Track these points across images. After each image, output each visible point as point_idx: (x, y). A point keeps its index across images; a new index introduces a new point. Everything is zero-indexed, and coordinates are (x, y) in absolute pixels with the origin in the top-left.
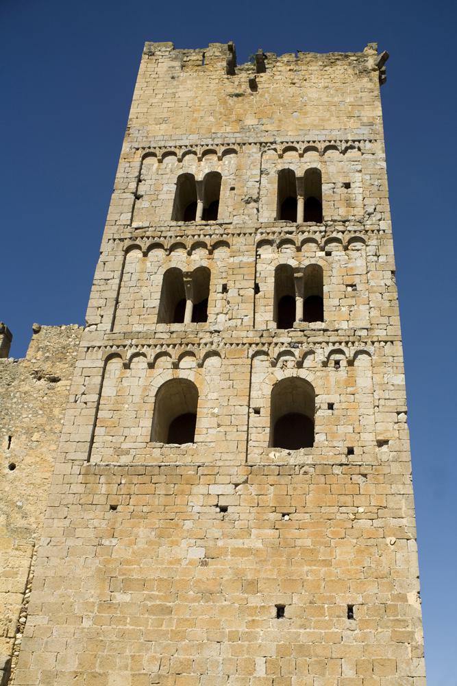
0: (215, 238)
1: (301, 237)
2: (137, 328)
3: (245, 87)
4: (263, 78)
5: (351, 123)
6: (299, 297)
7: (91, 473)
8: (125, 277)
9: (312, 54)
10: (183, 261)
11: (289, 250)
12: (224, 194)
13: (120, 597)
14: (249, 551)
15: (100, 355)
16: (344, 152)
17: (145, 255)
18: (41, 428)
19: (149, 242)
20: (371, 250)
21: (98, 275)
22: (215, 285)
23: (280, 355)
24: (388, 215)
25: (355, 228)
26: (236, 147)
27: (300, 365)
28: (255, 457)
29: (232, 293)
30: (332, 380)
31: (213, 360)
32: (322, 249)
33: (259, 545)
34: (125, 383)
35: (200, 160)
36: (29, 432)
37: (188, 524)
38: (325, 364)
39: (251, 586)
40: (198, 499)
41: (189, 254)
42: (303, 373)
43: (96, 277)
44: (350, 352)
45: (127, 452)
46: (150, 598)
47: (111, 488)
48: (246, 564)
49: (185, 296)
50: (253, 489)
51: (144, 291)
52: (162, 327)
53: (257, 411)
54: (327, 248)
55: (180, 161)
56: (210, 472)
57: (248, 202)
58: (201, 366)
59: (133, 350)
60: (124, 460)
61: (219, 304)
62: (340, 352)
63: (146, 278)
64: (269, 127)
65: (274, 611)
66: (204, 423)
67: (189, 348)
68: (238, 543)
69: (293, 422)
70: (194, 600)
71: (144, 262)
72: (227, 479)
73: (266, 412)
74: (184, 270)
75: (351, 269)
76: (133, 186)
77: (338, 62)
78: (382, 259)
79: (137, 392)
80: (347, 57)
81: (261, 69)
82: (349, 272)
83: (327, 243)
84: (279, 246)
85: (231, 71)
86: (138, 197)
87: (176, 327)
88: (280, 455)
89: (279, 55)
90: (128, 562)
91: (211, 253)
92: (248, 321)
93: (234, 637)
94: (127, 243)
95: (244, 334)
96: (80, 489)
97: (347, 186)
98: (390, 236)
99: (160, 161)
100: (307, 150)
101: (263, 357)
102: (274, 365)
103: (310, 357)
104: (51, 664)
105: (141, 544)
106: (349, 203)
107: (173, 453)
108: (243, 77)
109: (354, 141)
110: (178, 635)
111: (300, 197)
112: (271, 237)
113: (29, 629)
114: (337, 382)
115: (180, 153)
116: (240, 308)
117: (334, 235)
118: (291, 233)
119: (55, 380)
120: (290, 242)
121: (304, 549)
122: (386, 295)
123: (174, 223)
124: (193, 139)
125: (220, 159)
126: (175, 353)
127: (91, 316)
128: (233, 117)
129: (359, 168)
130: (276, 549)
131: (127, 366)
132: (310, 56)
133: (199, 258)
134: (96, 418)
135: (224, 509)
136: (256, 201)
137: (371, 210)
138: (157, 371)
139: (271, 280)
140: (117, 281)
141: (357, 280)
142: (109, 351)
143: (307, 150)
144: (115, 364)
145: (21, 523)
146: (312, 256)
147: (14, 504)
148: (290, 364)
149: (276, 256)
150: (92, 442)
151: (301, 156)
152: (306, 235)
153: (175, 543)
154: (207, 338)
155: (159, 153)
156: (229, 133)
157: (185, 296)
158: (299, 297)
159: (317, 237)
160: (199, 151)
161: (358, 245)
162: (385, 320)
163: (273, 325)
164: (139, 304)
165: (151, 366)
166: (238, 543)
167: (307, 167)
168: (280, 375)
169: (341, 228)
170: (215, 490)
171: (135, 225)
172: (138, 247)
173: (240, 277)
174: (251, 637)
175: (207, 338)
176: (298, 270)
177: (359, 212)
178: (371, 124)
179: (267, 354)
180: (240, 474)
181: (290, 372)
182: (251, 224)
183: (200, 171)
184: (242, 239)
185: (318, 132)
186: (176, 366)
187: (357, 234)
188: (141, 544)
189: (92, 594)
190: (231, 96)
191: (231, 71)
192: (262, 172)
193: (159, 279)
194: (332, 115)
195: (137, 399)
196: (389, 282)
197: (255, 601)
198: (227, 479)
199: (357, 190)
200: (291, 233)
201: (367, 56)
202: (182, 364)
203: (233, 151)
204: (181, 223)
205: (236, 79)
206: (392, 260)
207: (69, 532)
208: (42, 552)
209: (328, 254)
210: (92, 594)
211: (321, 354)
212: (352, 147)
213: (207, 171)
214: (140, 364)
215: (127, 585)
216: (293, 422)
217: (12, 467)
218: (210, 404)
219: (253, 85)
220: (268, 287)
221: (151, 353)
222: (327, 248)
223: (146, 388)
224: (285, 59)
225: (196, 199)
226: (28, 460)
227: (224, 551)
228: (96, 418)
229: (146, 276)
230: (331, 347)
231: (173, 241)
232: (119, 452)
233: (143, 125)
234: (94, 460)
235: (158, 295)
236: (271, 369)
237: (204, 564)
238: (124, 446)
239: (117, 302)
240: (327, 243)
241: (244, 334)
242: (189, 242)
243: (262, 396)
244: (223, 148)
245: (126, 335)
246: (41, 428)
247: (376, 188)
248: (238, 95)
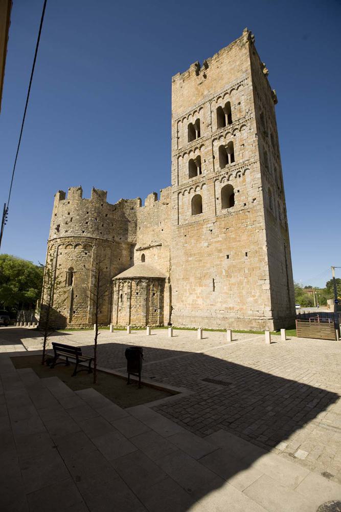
0: (201, 144)
1: (225, 133)
2: (184, 182)
3: (203, 78)
4: (208, 72)
5: (239, 74)
6: (226, 154)
7: (179, 228)
8: (179, 167)
9: (223, 49)
10: (193, 156)
11: (222, 139)
12: (202, 126)
13: (190, 259)
14: (218, 241)
15: (176, 194)
16: (237, 89)
17: (183, 157)
18: (166, 218)
19: (183, 153)
20: (248, 127)
21: (172, 169)
22: (202, 161)
23: (222, 178)
24: (254, 110)
25: (243, 121)
26: (202, 106)
27: (228, 180)
28: (218, 213)
29: (207, 162)
30: (238, 182)
31: (204, 186)
32: (232, 134)
33: (221, 239)
34: (184, 200)
35: (193, 116)
36: (164, 220)
37: (203, 237)
38: (236, 177)
39: (220, 251)
40: (205, 230)
41: (194, 152)
42: (230, 183)
43: (172, 169)
44: (242, 171)
45: (187, 220)
46: (196, 258)
47: (186, 231)
48: (218, 245)
49: (195, 167)
50: (218, 223)
51: (184, 170)
52: (191, 180)
53: (218, 199)
54: (234, 133)
55: (187, 119)
56: (206, 221)
57: (208, 126)
58: (201, 189)
59: (184, 190)
60: (187, 222)
61: (204, 167)
62: (240, 171)
63: (184, 163)
64: (211, 92)
65: (226, 257)
66: (204, 206)
67: (197, 185)
68: (215, 240)
69: (229, 197)
70: (207, 257)
71: (183, 160)
72: (211, 222)
73: (220, 199)
74: (194, 159)
75: (242, 138)
76: (176, 135)
77: (233, 47)
78: (252, 130)
79: (187, 202)
80: (236, 42)
81: (207, 67)
82: (241, 140)
83: (233, 132)
84: (219, 139)
85: (198, 74)
86: (178, 138)
87: (194, 178)
88: (225, 211)
89: (212, 57)
90: (190, 250)
91: (200, 150)
92: (212, 170)
93: (217, 265)
94: (178, 155)
95: (211, 175)
96: (177, 232)
97: (239, 103)
98: (255, 119)
99: (182, 122)
100: (224, 95)
101: (218, 181)
102: (221, 182)
103: (231, 176)
104: (178, 277)
105: (193, 245)
106: (240, 111)
107: (198, 217)
108: (202, 74)
109: (240, 82)
110: (204, 266)
111: (224, 115)
112: (216, 137)
113: (172, 269)
114: (240, 182)
115: (187, 116)
116: (210, 167)
117: (236, 127)
118: (222, 132)
119: (168, 204)
120: (222, 136)
121: (233, 238)
122: (254, 145)
123: (189, 143)
124: (190, 109)
125: (199, 113)
126: (194, 187)
127: (173, 183)
128: (200, 94)
129: (243, 94)
130: (226, 239)
131: (183, 195)
132: (223, 51)
133: (197, 153)
134: (178, 212)
135: (211, 231)
136: (211, 125)
137: (247, 111)
138: (191, 194)
139: (218, 153)
140: (177, 169)
141: (244, 142)
142: (178, 192)
143: (224, 95)
144: (181, 195)
145: (166, 244)
146: (230, 138)
147: (164, 239)
148: (226, 180)
149: (218, 143)
150: (178, 219)
151: (223, 99)
152: (227, 131)
153: (201, 243)
154: (202, 180)
155: (181, 119)
156: (200, 101)
157: (195, 167)
158: (226, 154)
159: (230, 131)
160: (192, 113)
161: (244, 127)
162: (253, 155)
163: (220, 168)
164: (184, 175)
165: (189, 193)
166: (215, 240)
167: (225, 102)
168: (223, 185)
169: (238, 123)
170: (209, 226)
171: (179, 149)
172: (181, 156)
173: (208, 156)
174: (221, 265)
175: (202, 180)
176: (226, 145)
177: (244, 113)
178: (247, 70)
179: (218, 179)
180: (214, 220)
181: (226, 183)
182: (210, 134)
183: (193, 120)
184: (208, 141)
185: (228, 85)
186: (195, 191)
187: (243, 124)
188: (193, 245)
189: (184, 259)
190: (199, 85)
191: (198, 74)
192: (211, 112)
193: (187, 164)
194: (232, 75)
195: (187, 204)
196: (255, 139)
197: (221, 255)
198: (211, 222)
199: (243, 104)
200: (222, 132)
201: (243, 37)
202: (197, 190)
203: (202, 108)
204: (191, 142)
205: (199, 76)
206: (255, 129)
207: (177, 244)
208: (172, 250)
209: (235, 135)
210: (184, 259)
211: (234, 174)
212: (240, 86)
213: (196, 119)
214: (186, 193)
215: (191, 255)
216: (229, 197)
217: (162, 230)
218: (205, 200)
219: (205, 76)
220: (217, 155)
221: (188, 189)
222: (234, 133)
223: (189, 200)
224: (214, 58)
225: (194, 131)
226: (165, 227)
227: (212, 243)
228: (178, 212)
229: (184, 165)
230: (237, 171)
231: (189, 150)
232: (185, 220)
233: (176, 111)
234: (180, 223)
235: (188, 170)
236: (220, 184)
237: (208, 247)
238: (186, 218)
239: (178, 175)
240: (233, 132)
241: (211, 175)
242: (193, 149)
243: (219, 194)
244: (199, 108)
245: (182, 186)
246: (166, 218)
247: (248, 100)
248: (201, 84)
